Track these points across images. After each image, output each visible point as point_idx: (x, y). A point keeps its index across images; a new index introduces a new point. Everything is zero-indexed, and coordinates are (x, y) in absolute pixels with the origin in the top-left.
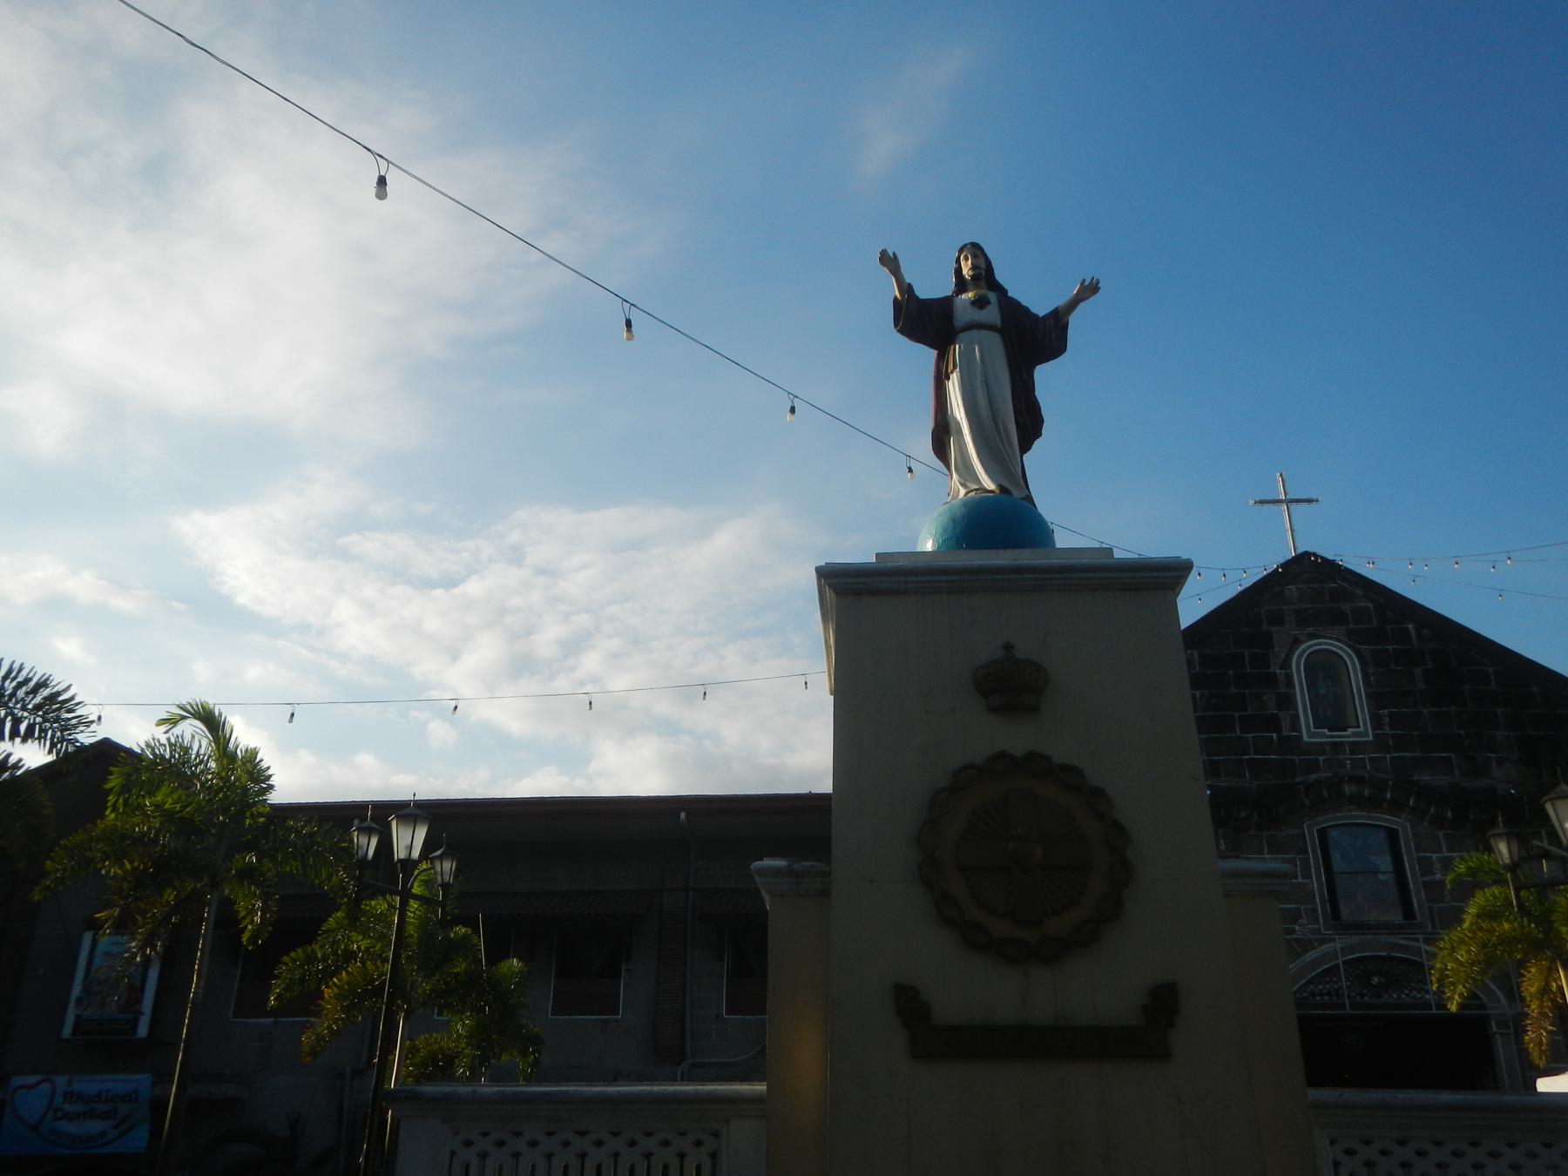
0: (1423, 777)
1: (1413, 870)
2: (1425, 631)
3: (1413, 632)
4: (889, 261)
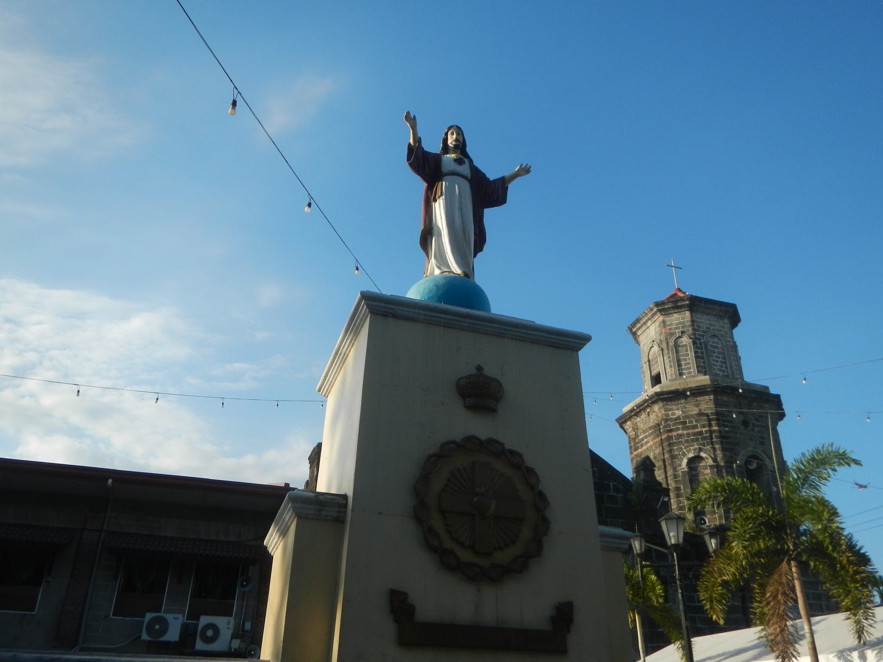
4: (411, 120)
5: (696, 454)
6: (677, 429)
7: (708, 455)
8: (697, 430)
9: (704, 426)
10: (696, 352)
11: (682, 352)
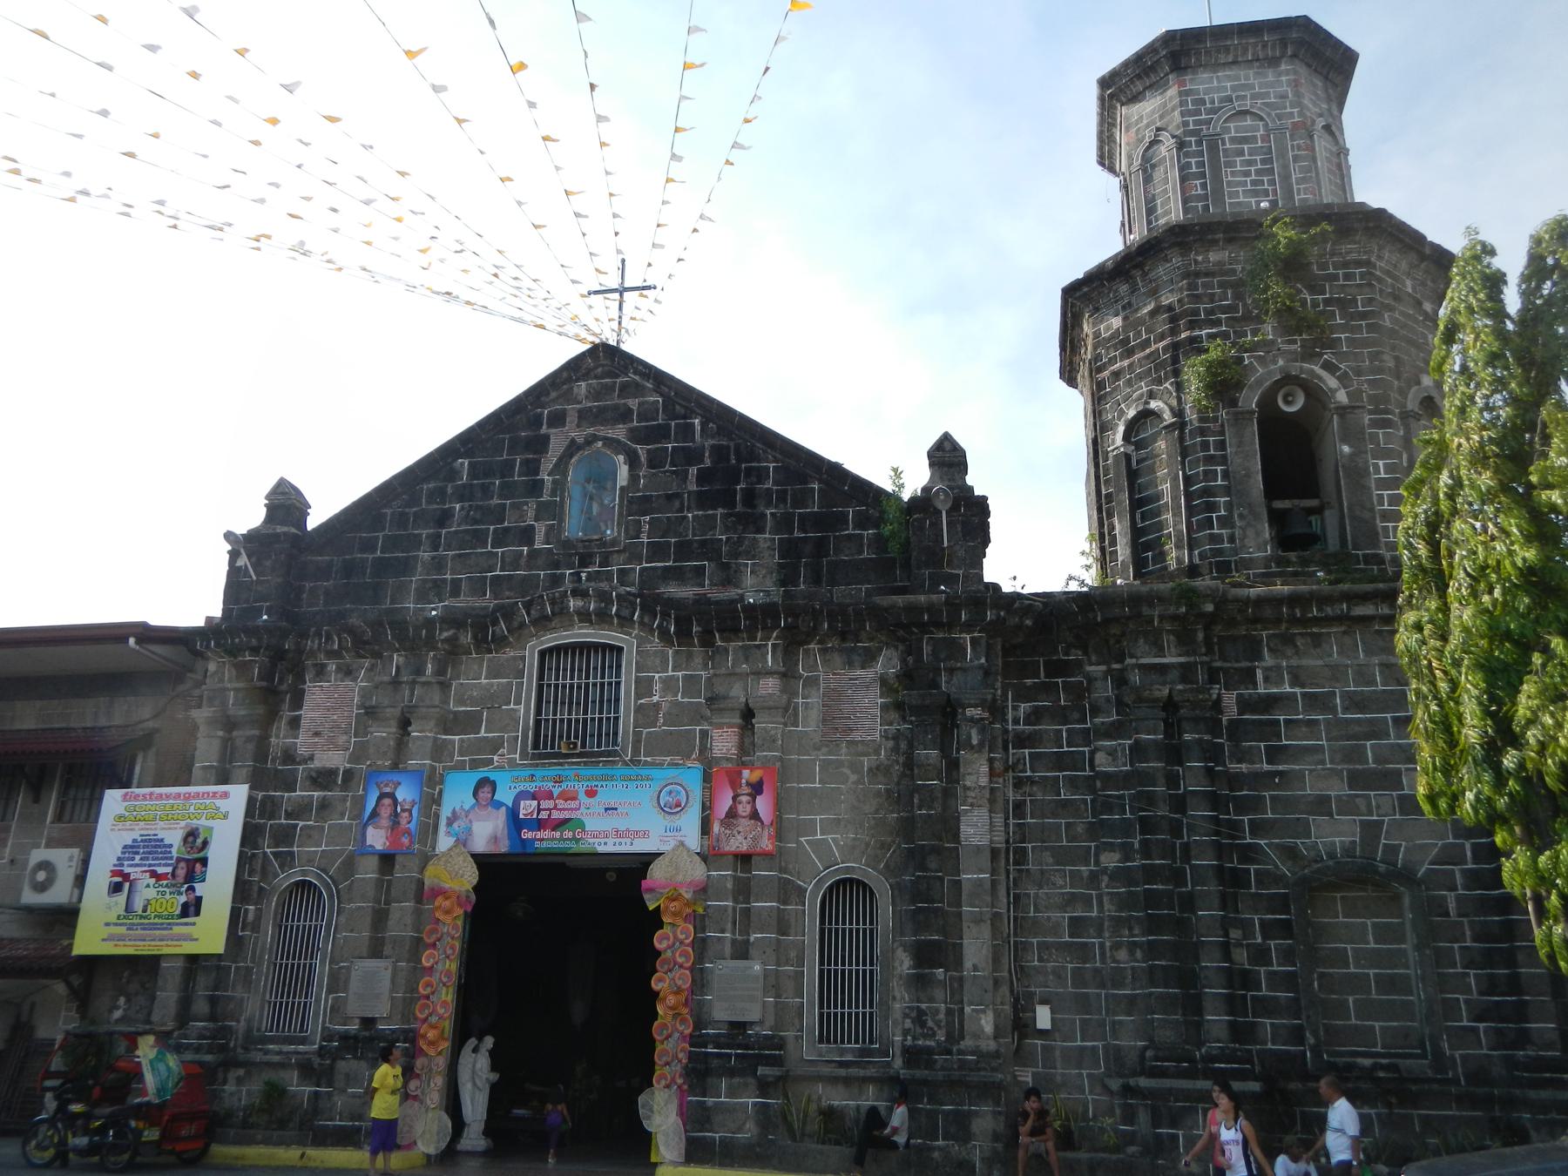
0: (674, 590)
1: (628, 693)
2: (711, 425)
3: (698, 428)
5: (1141, 408)
6: (1112, 361)
7: (1166, 404)
8: (1148, 351)
9: (1162, 337)
10: (1181, 169)
11: (1158, 175)
